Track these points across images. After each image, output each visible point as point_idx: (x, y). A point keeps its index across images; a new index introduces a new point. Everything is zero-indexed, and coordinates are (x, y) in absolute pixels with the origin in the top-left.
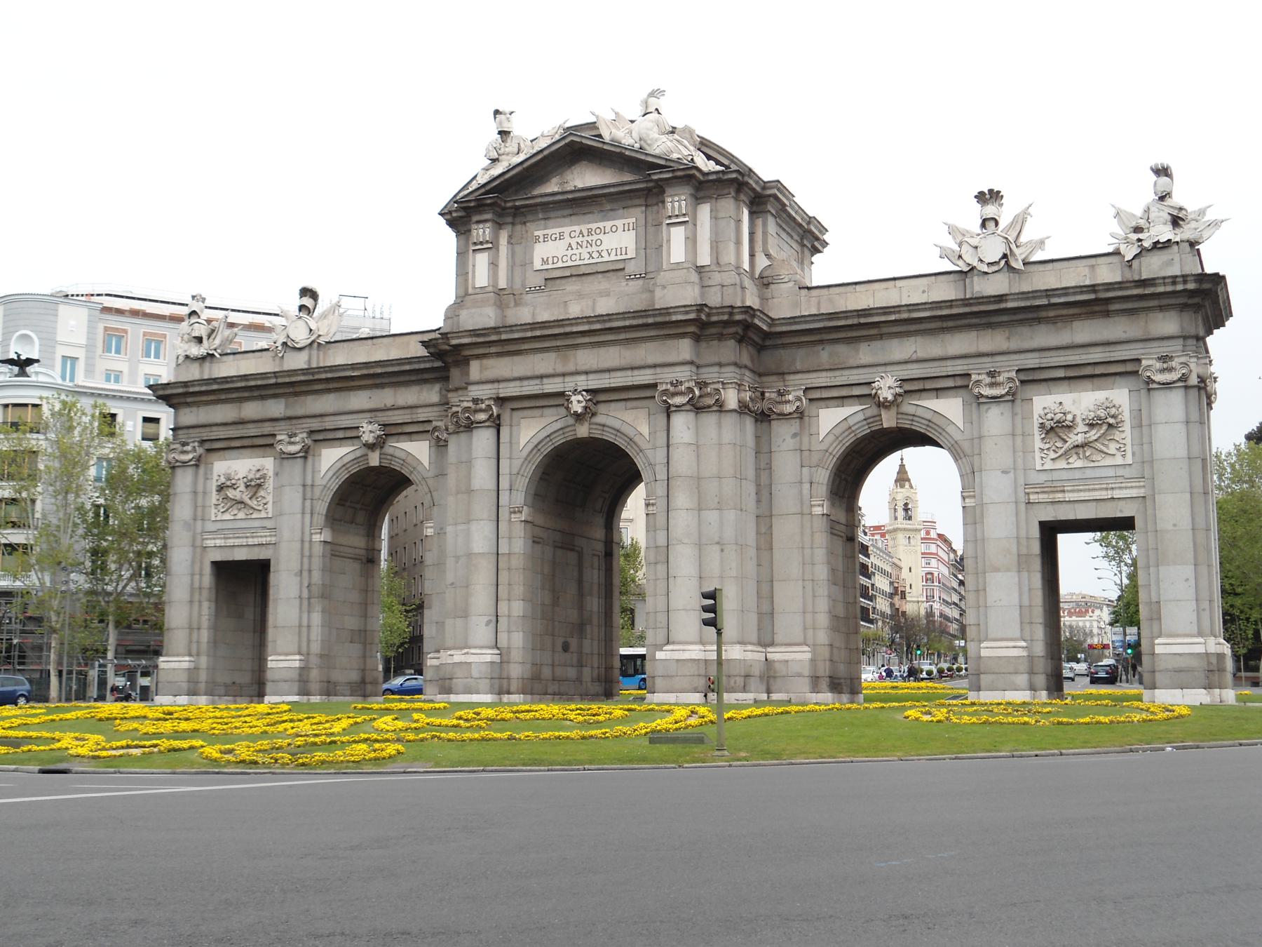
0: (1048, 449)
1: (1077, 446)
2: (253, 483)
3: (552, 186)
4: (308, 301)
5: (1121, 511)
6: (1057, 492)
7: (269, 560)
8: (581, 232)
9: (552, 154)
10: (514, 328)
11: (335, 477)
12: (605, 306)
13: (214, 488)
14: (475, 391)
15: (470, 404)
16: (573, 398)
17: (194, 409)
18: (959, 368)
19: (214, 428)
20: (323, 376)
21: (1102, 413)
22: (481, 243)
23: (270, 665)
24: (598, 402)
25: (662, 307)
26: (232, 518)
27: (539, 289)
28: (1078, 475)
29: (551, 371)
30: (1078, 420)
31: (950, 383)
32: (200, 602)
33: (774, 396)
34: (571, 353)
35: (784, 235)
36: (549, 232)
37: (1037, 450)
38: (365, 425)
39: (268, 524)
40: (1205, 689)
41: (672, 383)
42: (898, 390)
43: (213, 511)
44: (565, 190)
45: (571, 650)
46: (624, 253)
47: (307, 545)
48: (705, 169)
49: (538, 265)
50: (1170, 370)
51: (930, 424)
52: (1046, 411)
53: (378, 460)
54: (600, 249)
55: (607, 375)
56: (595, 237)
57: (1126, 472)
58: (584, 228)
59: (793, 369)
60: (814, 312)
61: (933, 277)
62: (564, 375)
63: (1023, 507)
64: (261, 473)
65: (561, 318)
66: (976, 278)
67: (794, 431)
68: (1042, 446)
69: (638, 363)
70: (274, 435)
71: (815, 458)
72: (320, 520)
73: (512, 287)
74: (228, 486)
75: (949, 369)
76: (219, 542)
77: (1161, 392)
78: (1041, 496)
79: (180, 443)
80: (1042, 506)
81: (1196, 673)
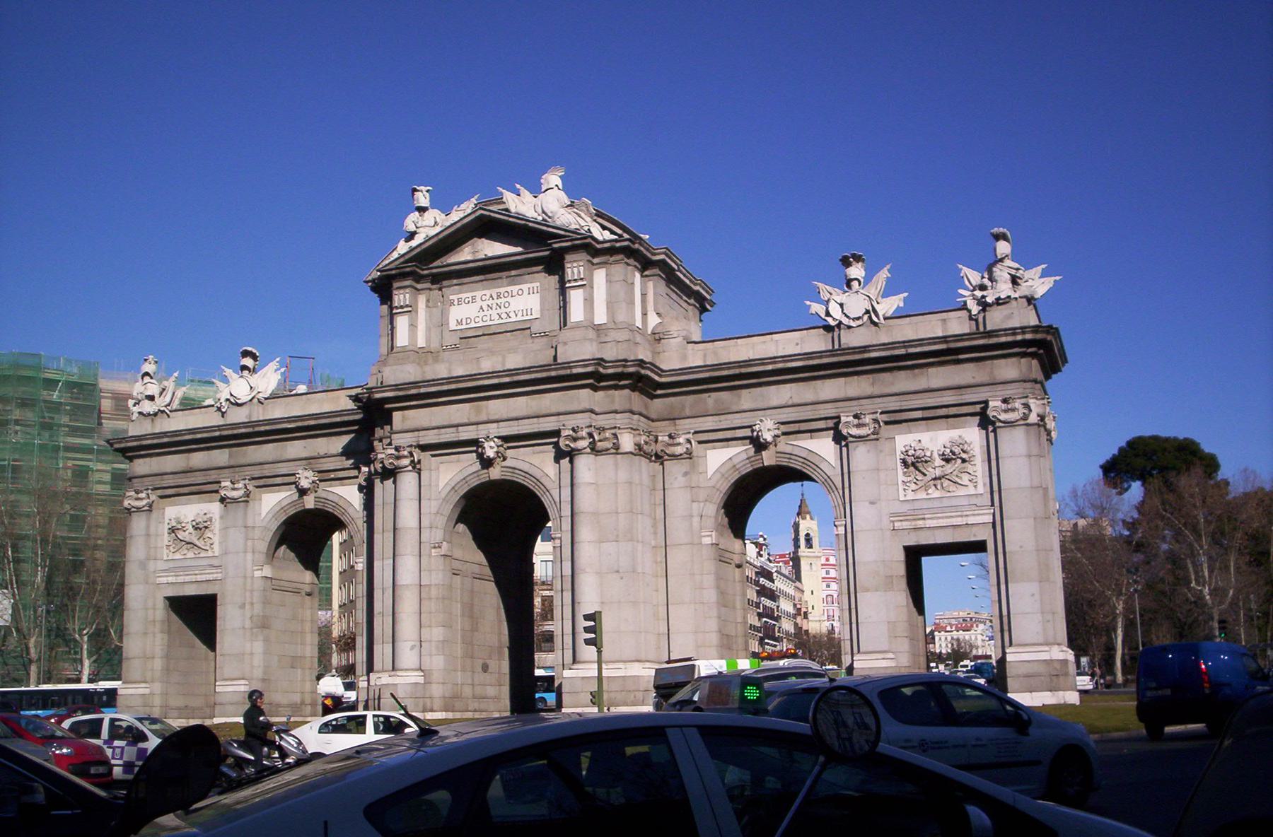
0: (910, 482)
1: (935, 479)
2: (201, 526)
3: (465, 254)
4: (248, 362)
5: (975, 535)
6: (919, 519)
9: (464, 227)
11: (274, 519)
12: (514, 362)
13: (166, 531)
14: (398, 440)
15: (393, 452)
16: (486, 445)
18: (830, 411)
20: (262, 428)
21: (953, 449)
22: (402, 307)
24: (509, 448)
25: (565, 361)
26: (183, 557)
27: (454, 348)
28: (936, 504)
29: (466, 421)
30: (936, 455)
31: (821, 424)
32: (154, 634)
33: (666, 439)
35: (674, 296)
36: (463, 296)
37: (900, 482)
38: (300, 472)
39: (216, 562)
40: (1051, 691)
41: (573, 430)
42: (777, 432)
43: (165, 551)
44: (476, 258)
45: (490, 670)
46: (529, 313)
47: (249, 580)
48: (600, 238)
49: (453, 326)
50: (1013, 410)
51: (806, 462)
52: (907, 448)
53: (313, 502)
54: (507, 310)
55: (515, 423)
56: (503, 300)
57: (978, 501)
58: (494, 292)
59: (683, 415)
60: (700, 363)
61: (805, 331)
62: (477, 424)
63: (888, 533)
64: (208, 516)
65: (473, 373)
67: (684, 470)
68: (906, 479)
69: (544, 412)
70: (219, 482)
71: (702, 495)
72: (261, 558)
73: (429, 346)
74: (178, 529)
75: (821, 412)
76: (171, 579)
77: (1008, 429)
78: (904, 523)
79: (135, 491)
80: (906, 532)
81: (1043, 678)
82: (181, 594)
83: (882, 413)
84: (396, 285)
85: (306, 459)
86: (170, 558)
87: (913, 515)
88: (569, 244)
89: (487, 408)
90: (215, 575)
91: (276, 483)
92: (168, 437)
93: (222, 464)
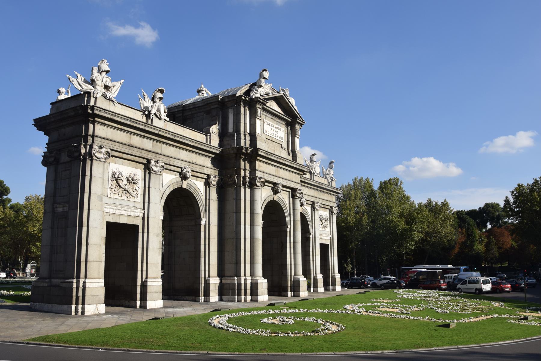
4: (159, 95)
7: (139, 225)
8: (274, 126)
10: (276, 156)
13: (110, 179)
17: (105, 128)
19: (117, 144)
22: (259, 116)
23: (149, 284)
26: (120, 198)
34: (279, 169)
36: (268, 121)
53: (186, 186)
56: (276, 130)
66: (315, 176)
76: (112, 211)
82: (118, 222)
83: (321, 204)
84: (258, 106)
85: (188, 162)
86: (112, 196)
87: (321, 234)
88: (300, 122)
89: (280, 172)
90: (138, 214)
91: (172, 169)
92: (131, 121)
93: (148, 149)
